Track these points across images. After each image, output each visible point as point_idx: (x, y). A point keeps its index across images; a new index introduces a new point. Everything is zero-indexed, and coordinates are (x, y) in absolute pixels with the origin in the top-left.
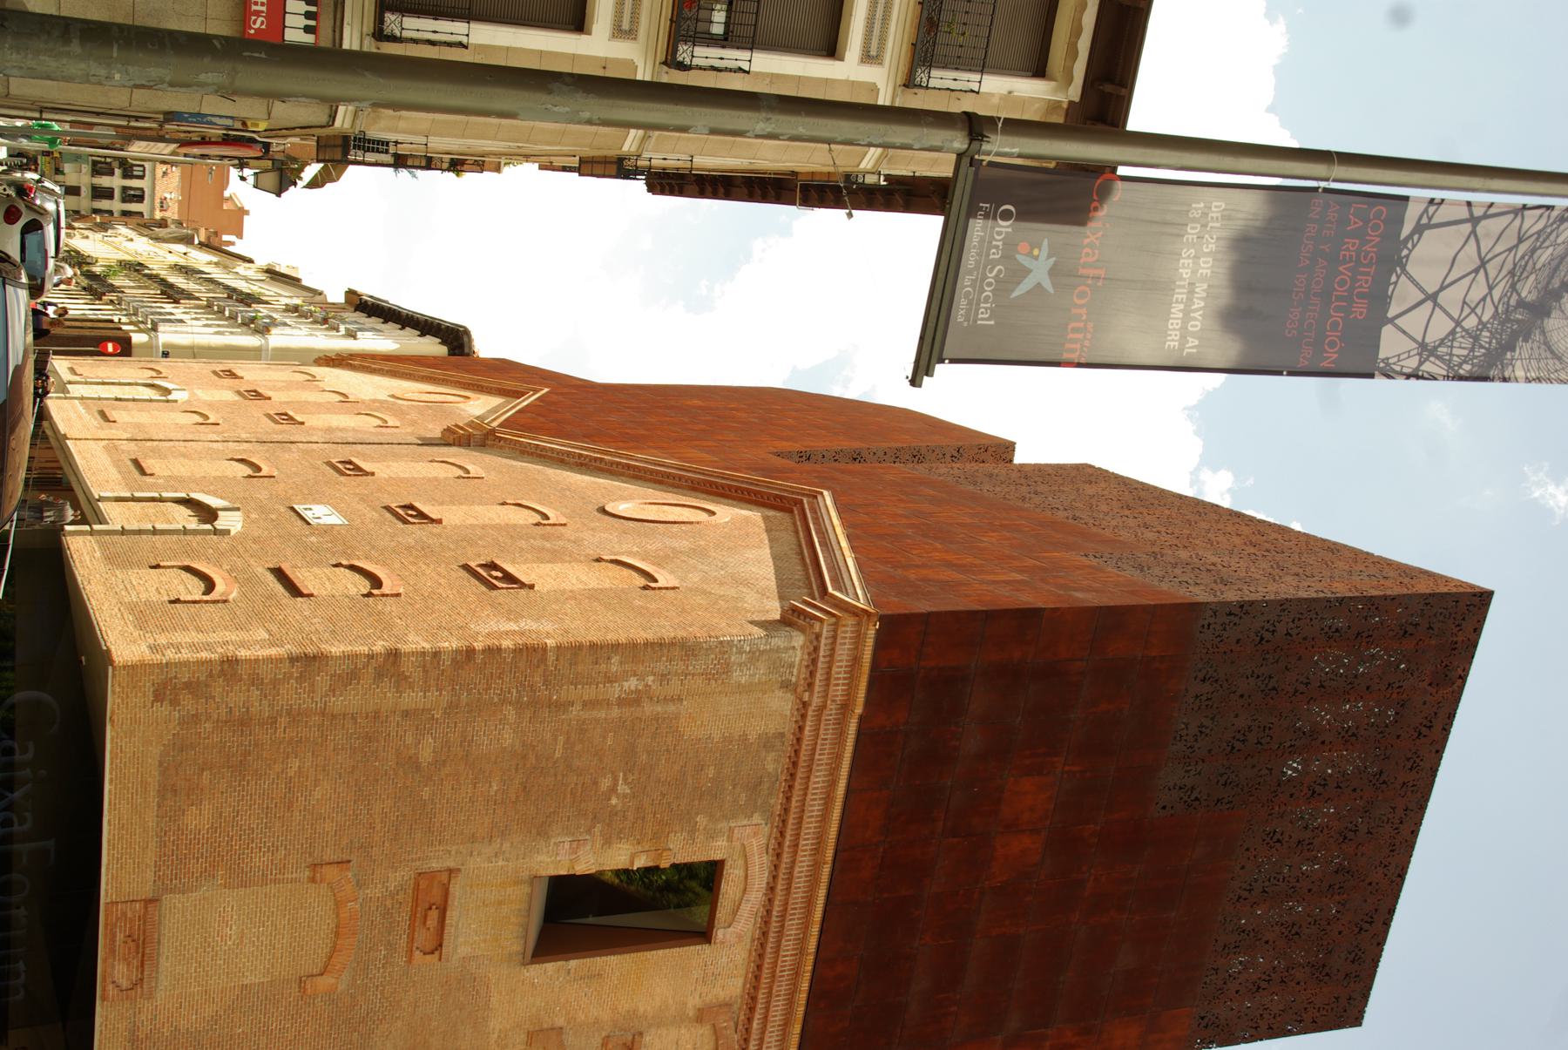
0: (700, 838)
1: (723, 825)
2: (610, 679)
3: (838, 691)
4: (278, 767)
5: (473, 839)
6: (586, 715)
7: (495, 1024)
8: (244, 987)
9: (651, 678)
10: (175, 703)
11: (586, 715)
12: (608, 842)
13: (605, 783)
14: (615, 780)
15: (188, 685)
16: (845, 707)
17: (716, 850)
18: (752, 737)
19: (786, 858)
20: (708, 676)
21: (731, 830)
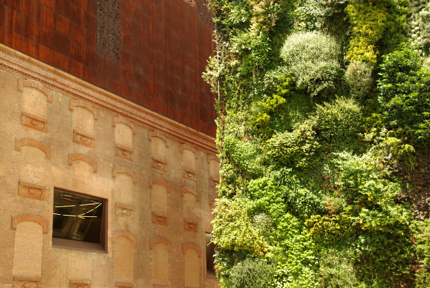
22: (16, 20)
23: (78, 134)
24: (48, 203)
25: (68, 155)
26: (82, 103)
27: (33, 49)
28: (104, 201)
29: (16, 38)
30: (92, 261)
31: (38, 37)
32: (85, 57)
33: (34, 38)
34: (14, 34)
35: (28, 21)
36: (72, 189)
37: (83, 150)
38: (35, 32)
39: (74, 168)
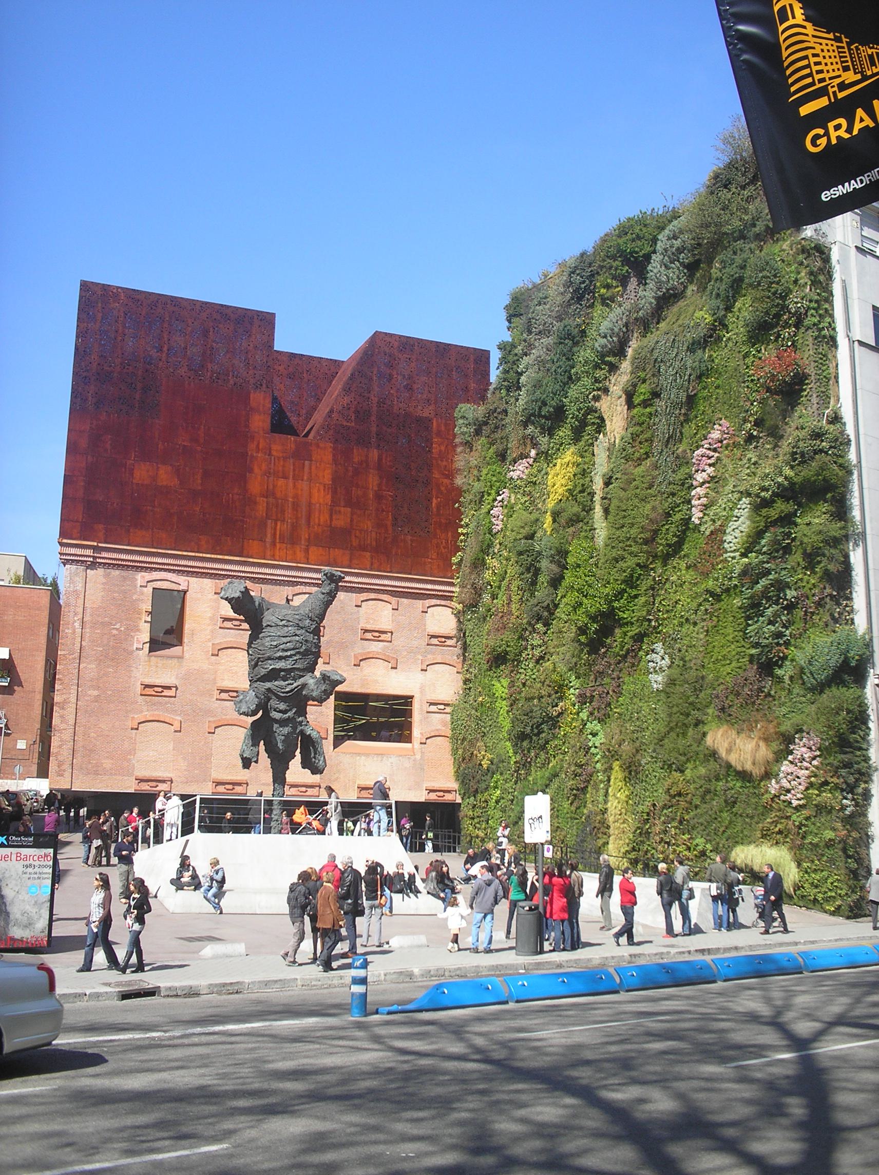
0: (141, 598)
1: (139, 589)
2: (74, 632)
3: (89, 552)
4: (93, 740)
5: (130, 677)
6: (87, 640)
7: (205, 666)
8: (174, 750)
9: (76, 618)
10: (64, 771)
11: (87, 640)
12: (138, 630)
13: (115, 632)
14: (114, 628)
15: (59, 767)
16: (95, 549)
17: (149, 590)
18: (104, 581)
19: (155, 566)
20: (78, 597)
21: (141, 586)
22: (280, 531)
23: (366, 631)
24: (327, 708)
25: (355, 655)
26: (373, 596)
27: (300, 554)
28: (407, 700)
29: (280, 549)
30: (389, 764)
31: (309, 540)
32: (374, 543)
33: (303, 542)
34: (278, 545)
35: (295, 527)
36: (360, 690)
37: (375, 647)
38: (304, 535)
39: (361, 669)
